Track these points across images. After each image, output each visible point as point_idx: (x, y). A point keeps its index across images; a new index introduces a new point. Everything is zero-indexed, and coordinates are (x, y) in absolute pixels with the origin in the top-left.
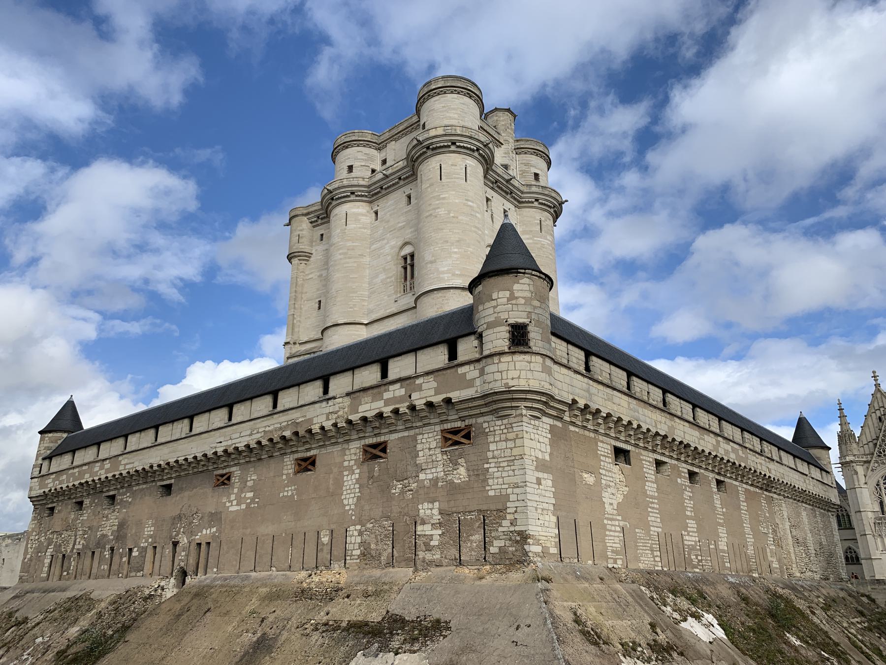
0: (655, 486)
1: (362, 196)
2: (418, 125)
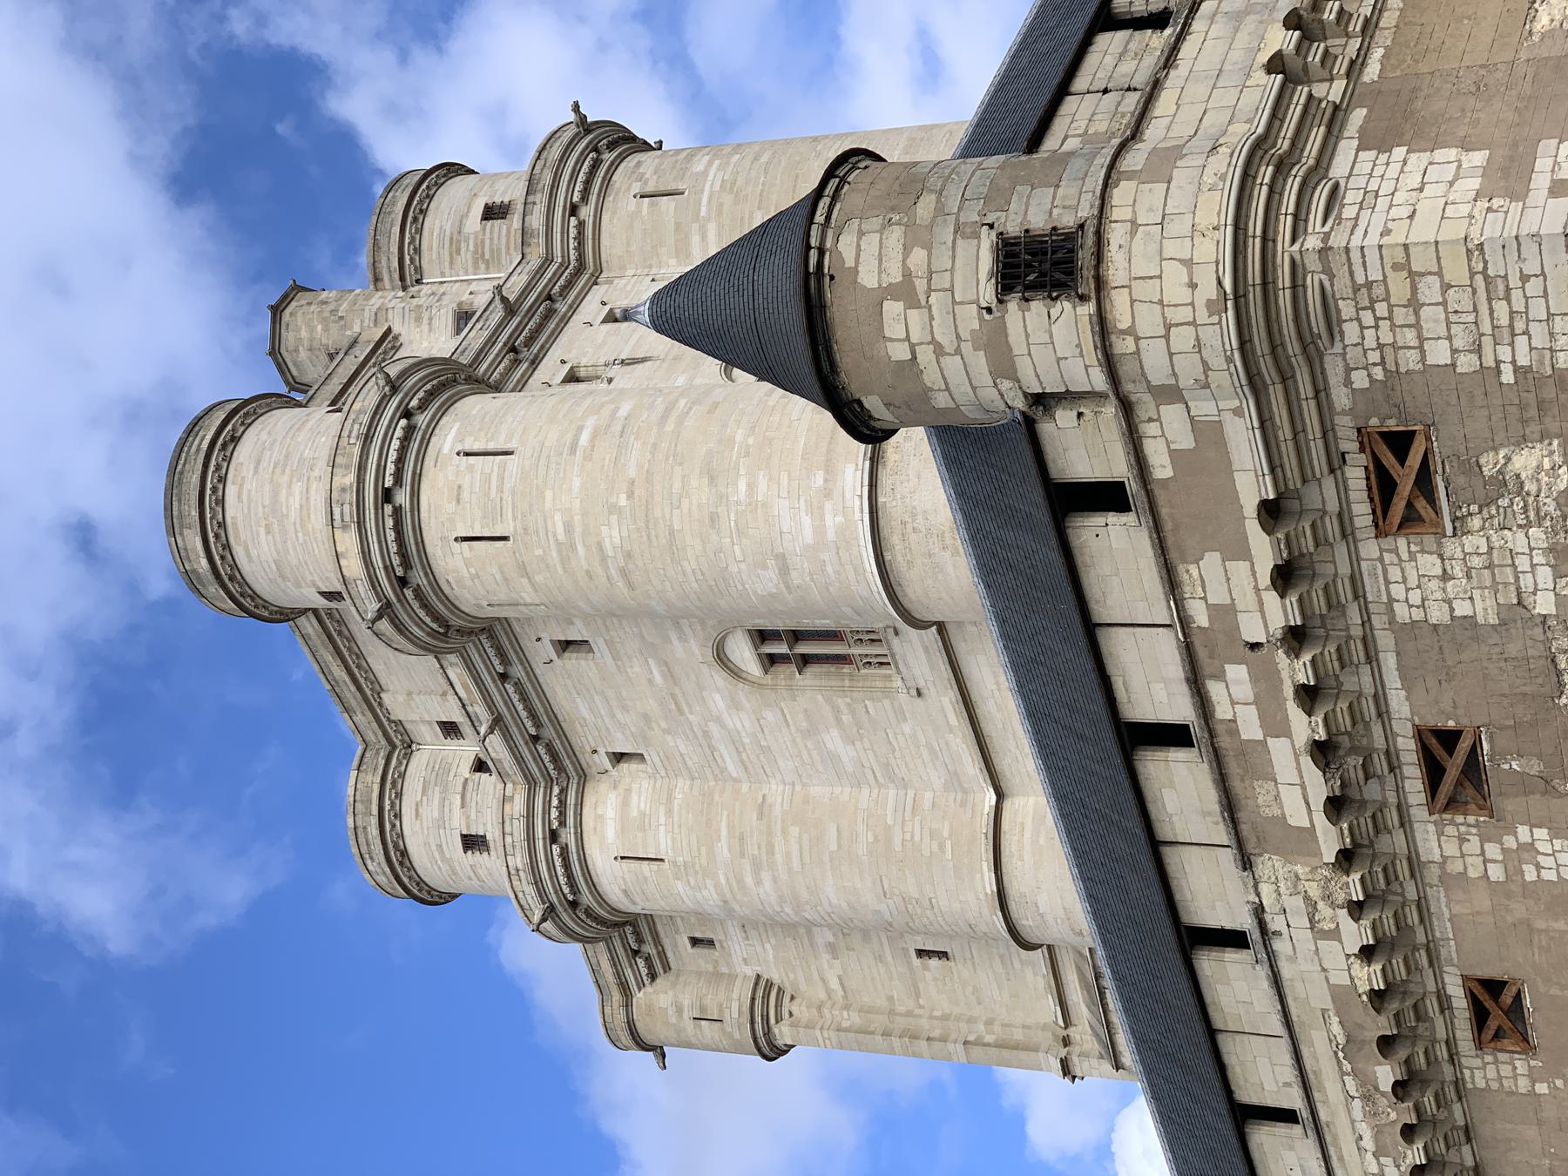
1: (562, 804)
2: (328, 619)
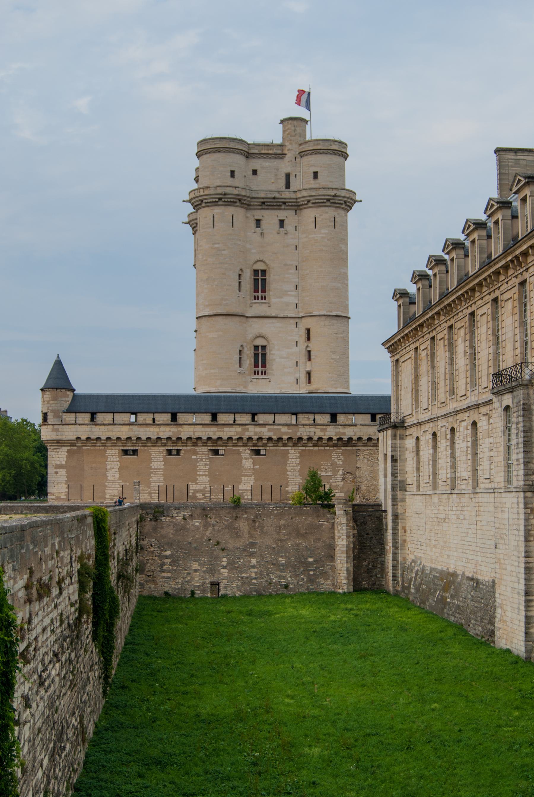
0: (163, 463)
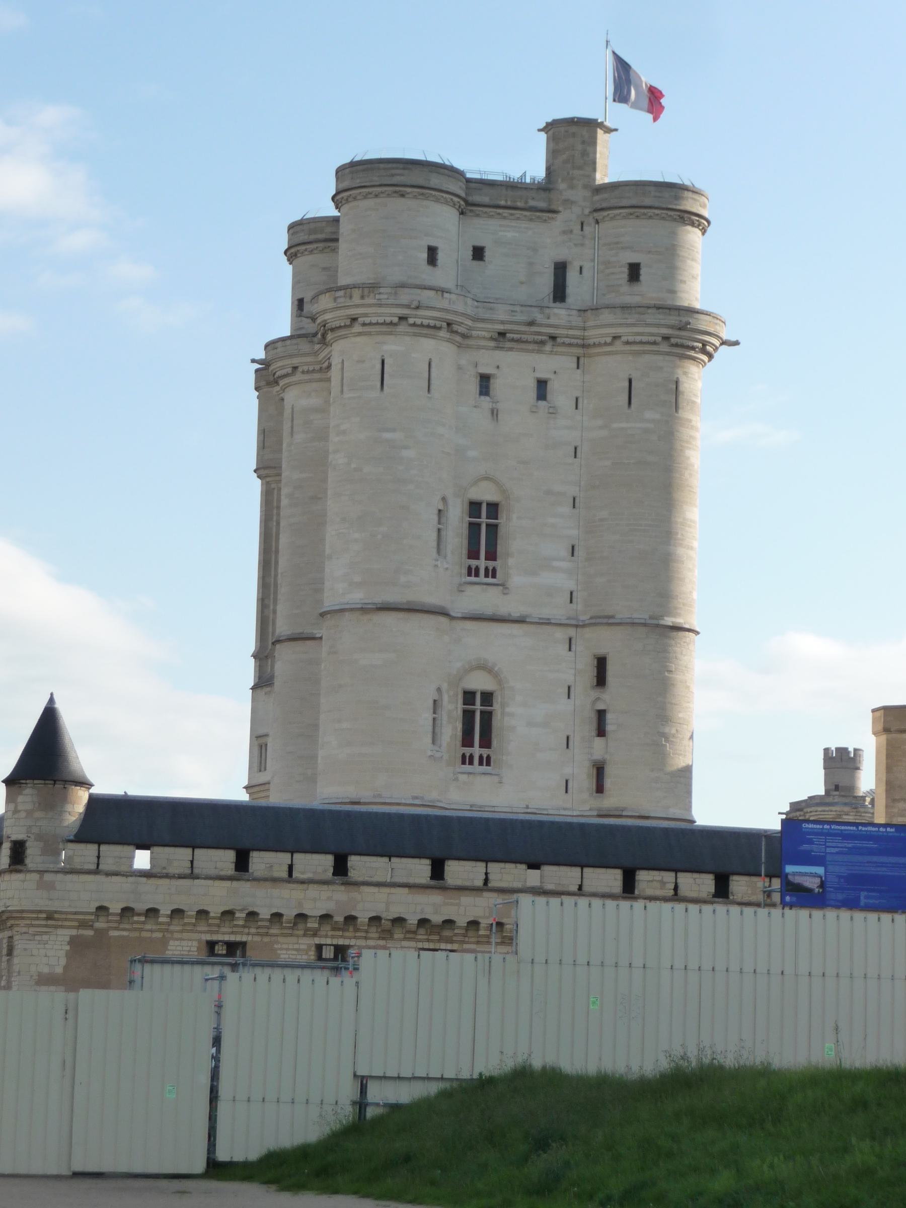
1: (313, 371)
